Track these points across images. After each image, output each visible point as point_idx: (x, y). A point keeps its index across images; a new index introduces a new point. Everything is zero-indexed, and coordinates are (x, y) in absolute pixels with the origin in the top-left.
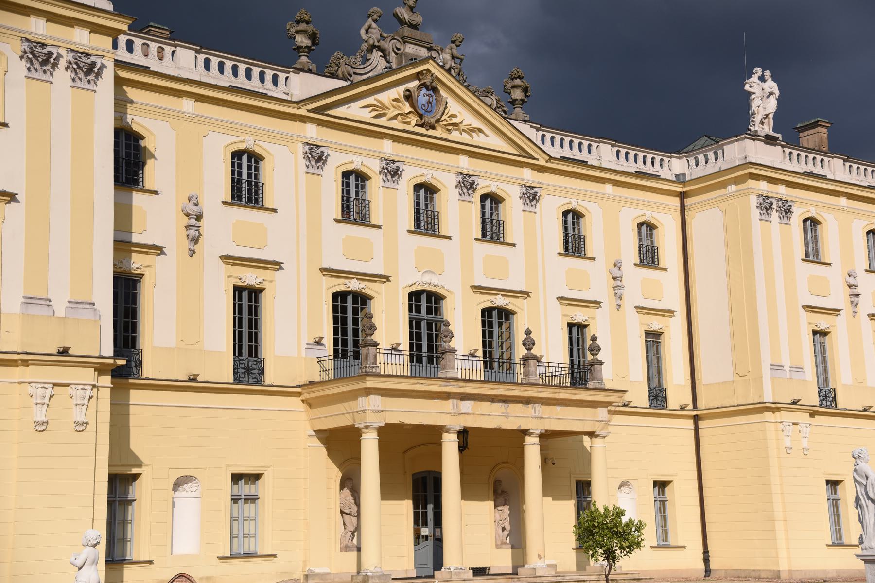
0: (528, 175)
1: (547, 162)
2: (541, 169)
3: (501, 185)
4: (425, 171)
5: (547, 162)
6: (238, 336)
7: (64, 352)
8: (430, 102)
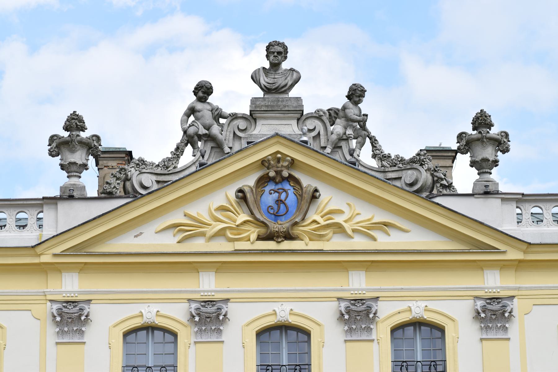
3: (432, 305)
4: (277, 307)
5: (525, 252)
8: (281, 201)
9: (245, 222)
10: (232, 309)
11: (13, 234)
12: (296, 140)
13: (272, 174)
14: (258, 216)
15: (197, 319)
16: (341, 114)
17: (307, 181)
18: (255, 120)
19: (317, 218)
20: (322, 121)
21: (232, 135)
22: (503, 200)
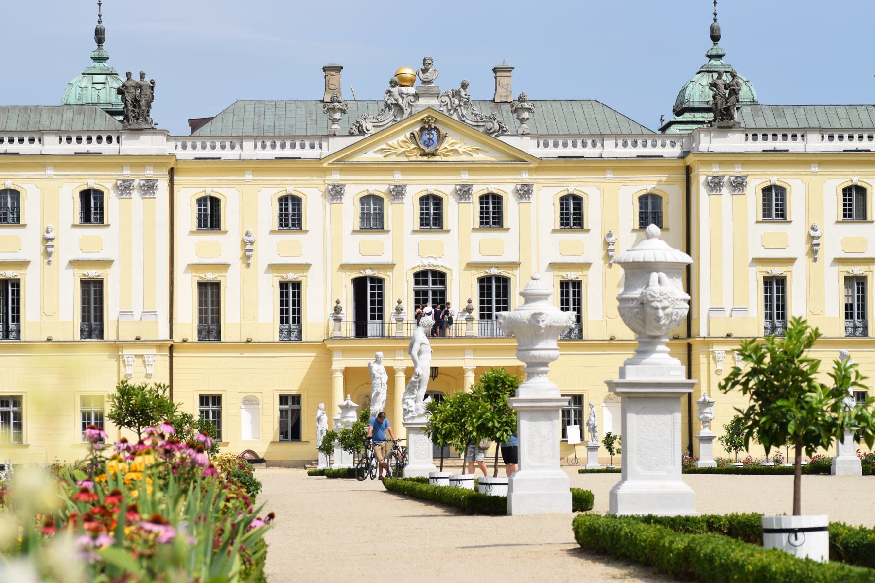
0: (525, 177)
1: (540, 163)
2: (537, 170)
4: (428, 187)
5: (540, 163)
6: (284, 312)
9: (414, 148)
10: (408, 189)
11: (308, 151)
12: (437, 109)
13: (427, 126)
14: (420, 146)
16: (458, 93)
18: (418, 97)
19: (447, 146)
20: (449, 97)
22: (531, 137)
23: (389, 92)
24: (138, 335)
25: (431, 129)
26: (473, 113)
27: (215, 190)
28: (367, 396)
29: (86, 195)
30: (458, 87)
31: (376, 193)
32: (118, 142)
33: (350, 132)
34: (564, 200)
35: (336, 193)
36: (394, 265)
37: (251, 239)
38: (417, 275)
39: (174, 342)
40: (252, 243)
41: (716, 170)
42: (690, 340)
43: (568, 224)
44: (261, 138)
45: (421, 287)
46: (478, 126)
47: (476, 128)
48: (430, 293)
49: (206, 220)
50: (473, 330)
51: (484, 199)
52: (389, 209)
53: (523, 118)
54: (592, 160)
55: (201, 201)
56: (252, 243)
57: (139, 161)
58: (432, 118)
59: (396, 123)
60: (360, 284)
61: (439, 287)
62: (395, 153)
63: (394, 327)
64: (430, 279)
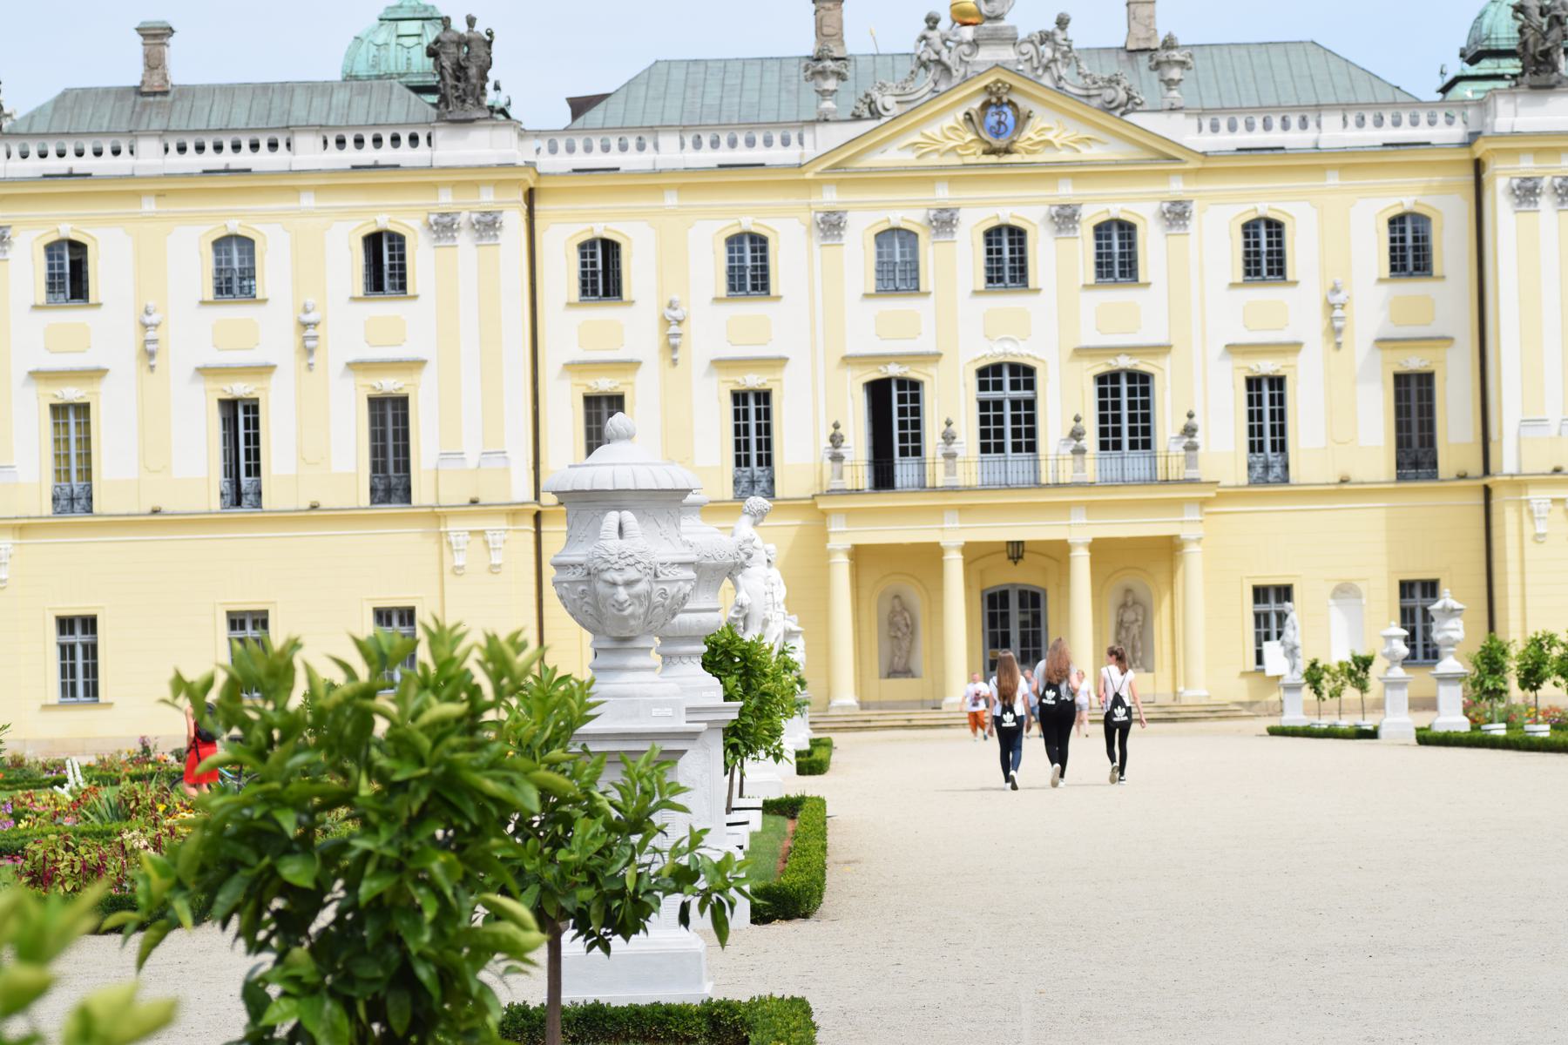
0: (1177, 188)
2: (1198, 172)
5: (1203, 162)
7: (474, 502)
9: (972, 141)
10: (963, 215)
13: (994, 100)
14: (983, 135)
15: (934, 224)
16: (1050, 38)
17: (1023, 104)
18: (978, 46)
19: (1031, 134)
21: (958, 60)
22: (1186, 114)
23: (924, 38)
24: (473, 496)
25: (1002, 104)
26: (1079, 74)
27: (610, 226)
28: (897, 596)
29: (374, 242)
30: (1050, 26)
31: (903, 225)
32: (430, 144)
33: (853, 115)
34: (1250, 229)
35: (831, 225)
36: (939, 355)
37: (677, 314)
38: (982, 372)
39: (542, 506)
40: (679, 322)
41: (1527, 166)
42: (1487, 481)
43: (1258, 273)
44: (692, 129)
45: (991, 395)
46: (1089, 96)
47: (1084, 100)
48: (1007, 406)
49: (595, 283)
50: (1084, 471)
51: (1102, 231)
52: (930, 253)
53: (1172, 80)
54: (1299, 153)
55: (586, 248)
56: (679, 322)
57: (468, 177)
58: (1004, 83)
59: (936, 94)
60: (878, 392)
61: (1022, 394)
62: (937, 150)
63: (940, 469)
64: (1007, 379)
